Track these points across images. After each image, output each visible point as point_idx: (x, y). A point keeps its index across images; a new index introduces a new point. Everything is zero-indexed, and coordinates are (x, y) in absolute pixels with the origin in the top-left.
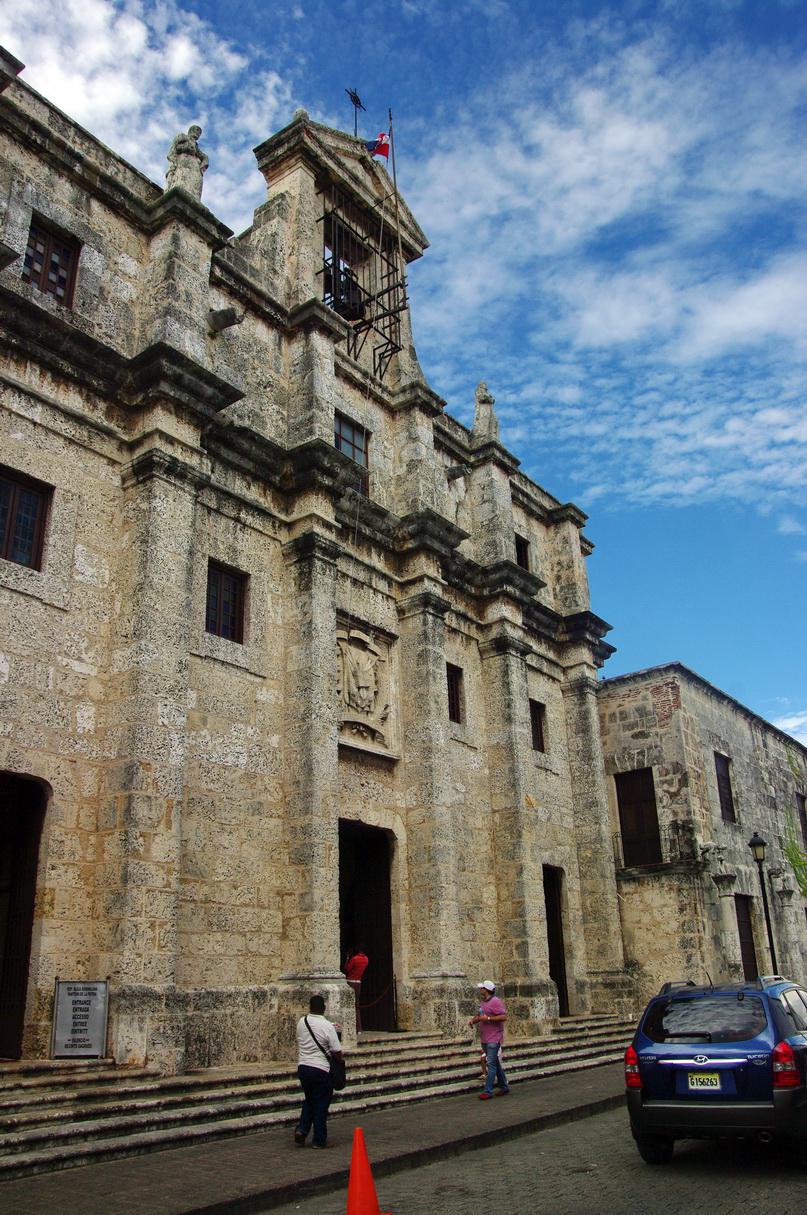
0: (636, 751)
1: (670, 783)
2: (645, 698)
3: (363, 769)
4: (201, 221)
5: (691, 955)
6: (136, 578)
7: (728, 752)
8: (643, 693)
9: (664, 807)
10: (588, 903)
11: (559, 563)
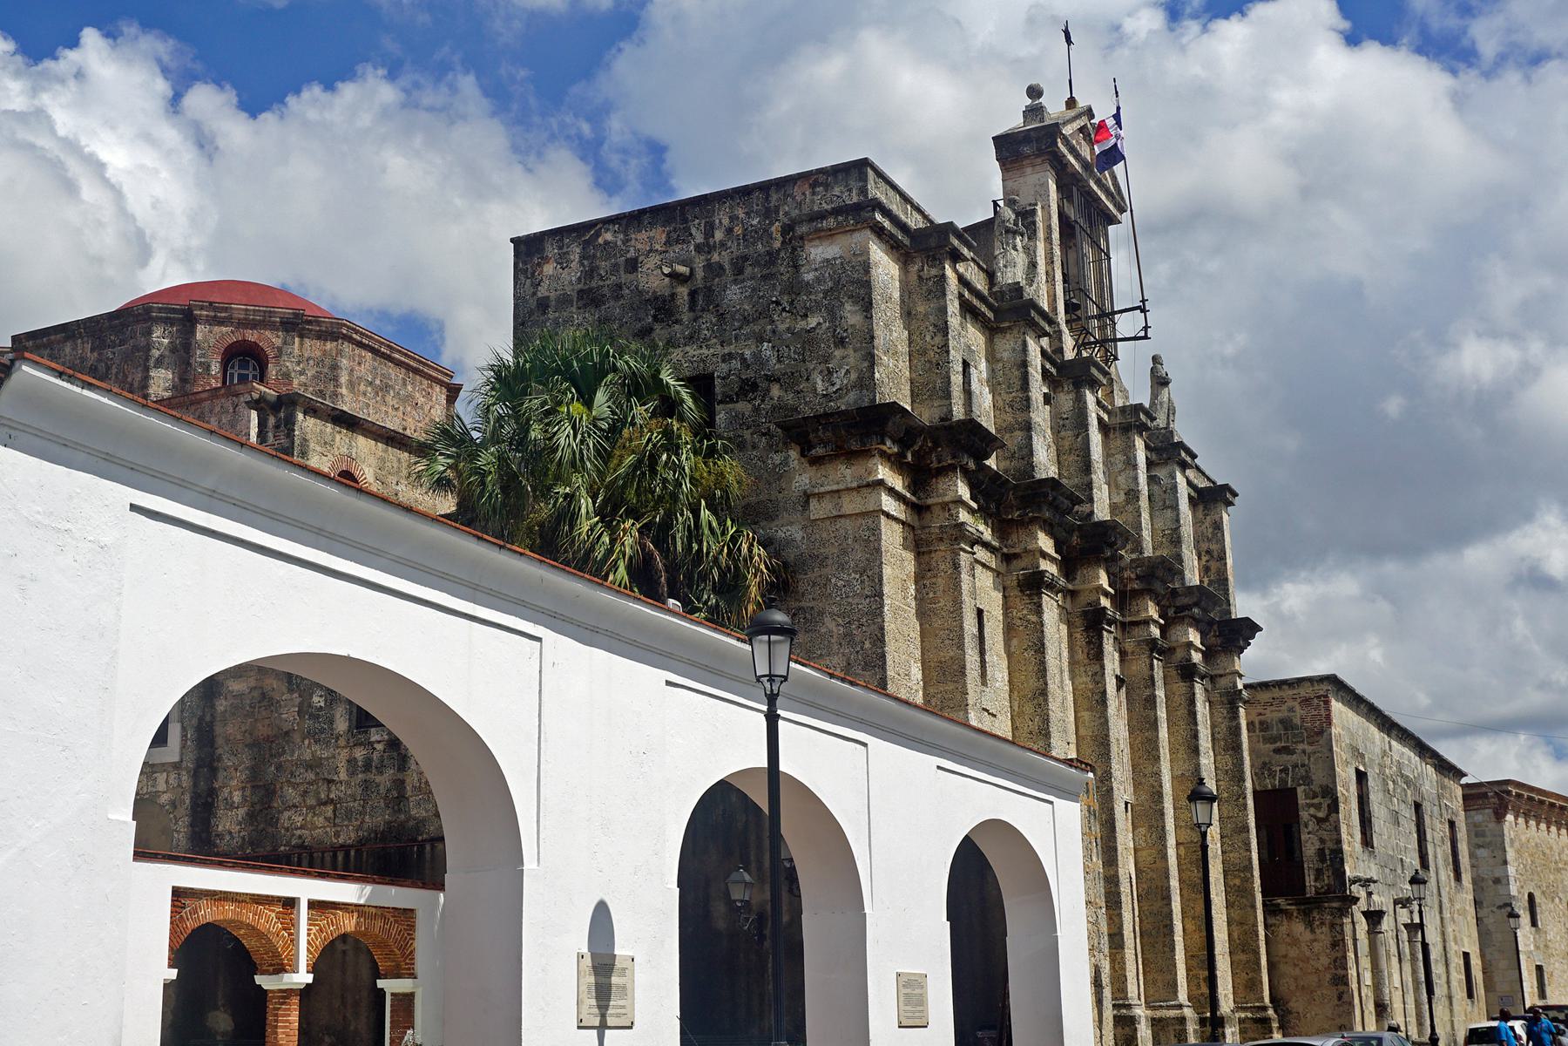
0: (1278, 769)
1: (1318, 807)
2: (1291, 710)
5: (1343, 993)
6: (1033, 683)
7: (1364, 765)
8: (1290, 703)
9: (1309, 833)
10: (1235, 935)
11: (1208, 552)
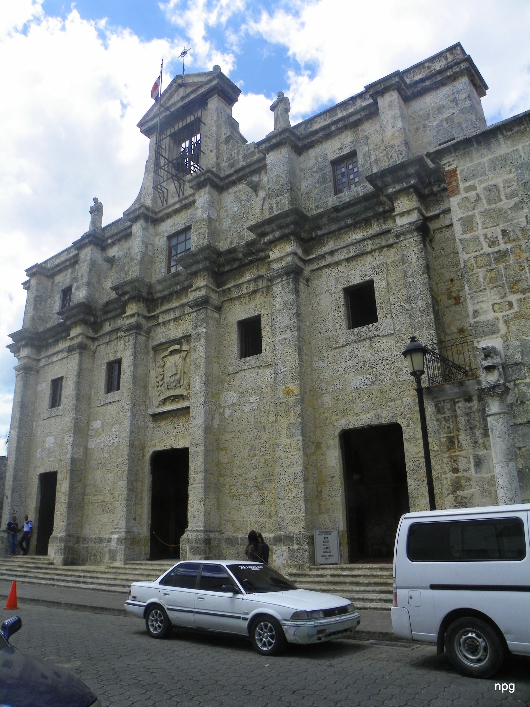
3: (175, 419)
4: (82, 243)
